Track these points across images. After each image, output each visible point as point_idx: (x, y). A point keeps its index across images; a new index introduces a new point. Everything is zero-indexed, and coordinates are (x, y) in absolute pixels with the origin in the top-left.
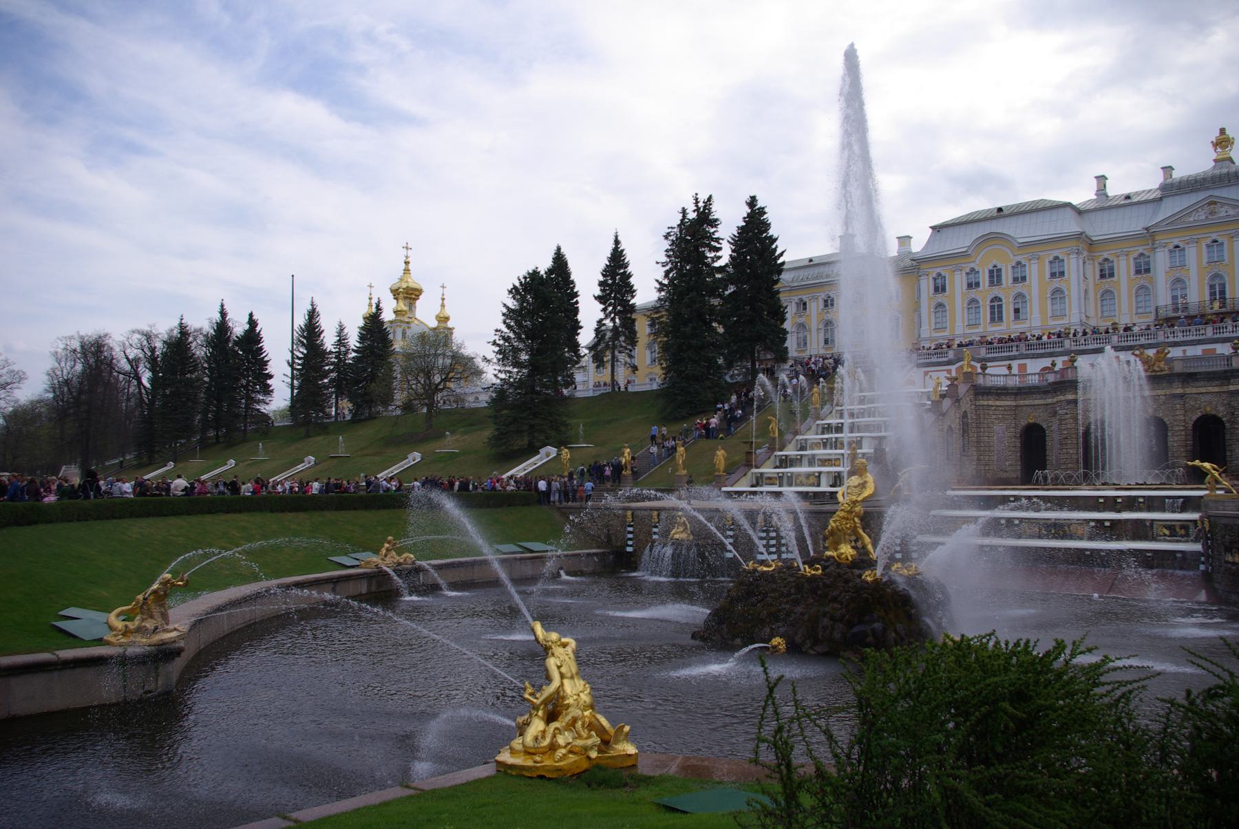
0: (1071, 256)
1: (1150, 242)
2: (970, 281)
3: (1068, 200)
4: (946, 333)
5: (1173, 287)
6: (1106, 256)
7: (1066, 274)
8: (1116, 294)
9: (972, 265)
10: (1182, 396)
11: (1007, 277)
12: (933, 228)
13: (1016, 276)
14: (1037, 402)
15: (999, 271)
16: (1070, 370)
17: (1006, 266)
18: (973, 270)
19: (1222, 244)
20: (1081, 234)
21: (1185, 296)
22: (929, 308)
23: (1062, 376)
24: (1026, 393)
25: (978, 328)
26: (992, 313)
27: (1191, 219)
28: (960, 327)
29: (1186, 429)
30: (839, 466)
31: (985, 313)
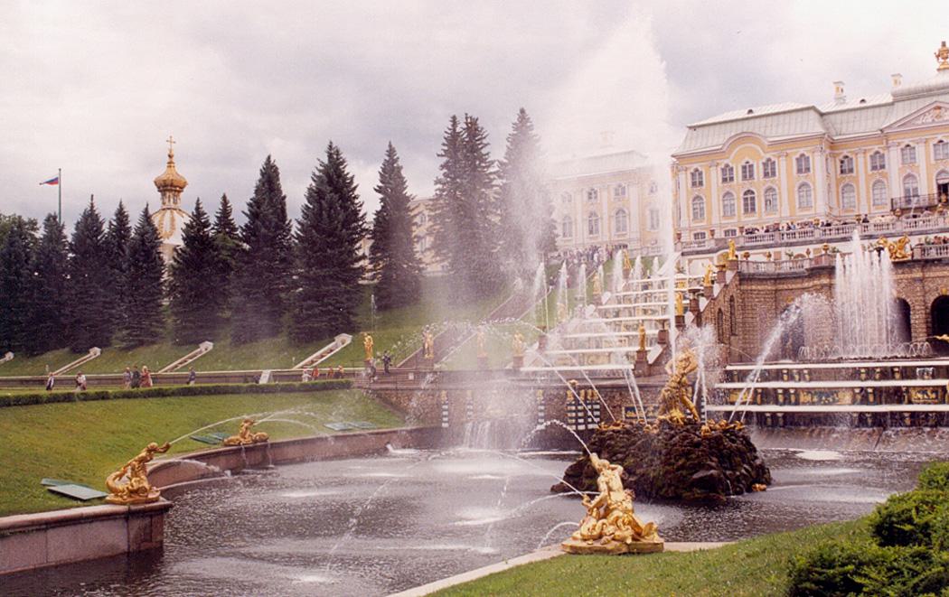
0: (816, 154)
1: (884, 141)
3: (811, 105)
7: (811, 170)
9: (726, 162)
10: (922, 280)
11: (758, 171)
12: (690, 128)
14: (794, 286)
15: (751, 166)
16: (823, 258)
17: (758, 164)
18: (727, 166)
20: (824, 134)
23: (817, 263)
26: (746, 205)
27: (920, 122)
28: (716, 219)
29: (927, 308)
31: (739, 205)
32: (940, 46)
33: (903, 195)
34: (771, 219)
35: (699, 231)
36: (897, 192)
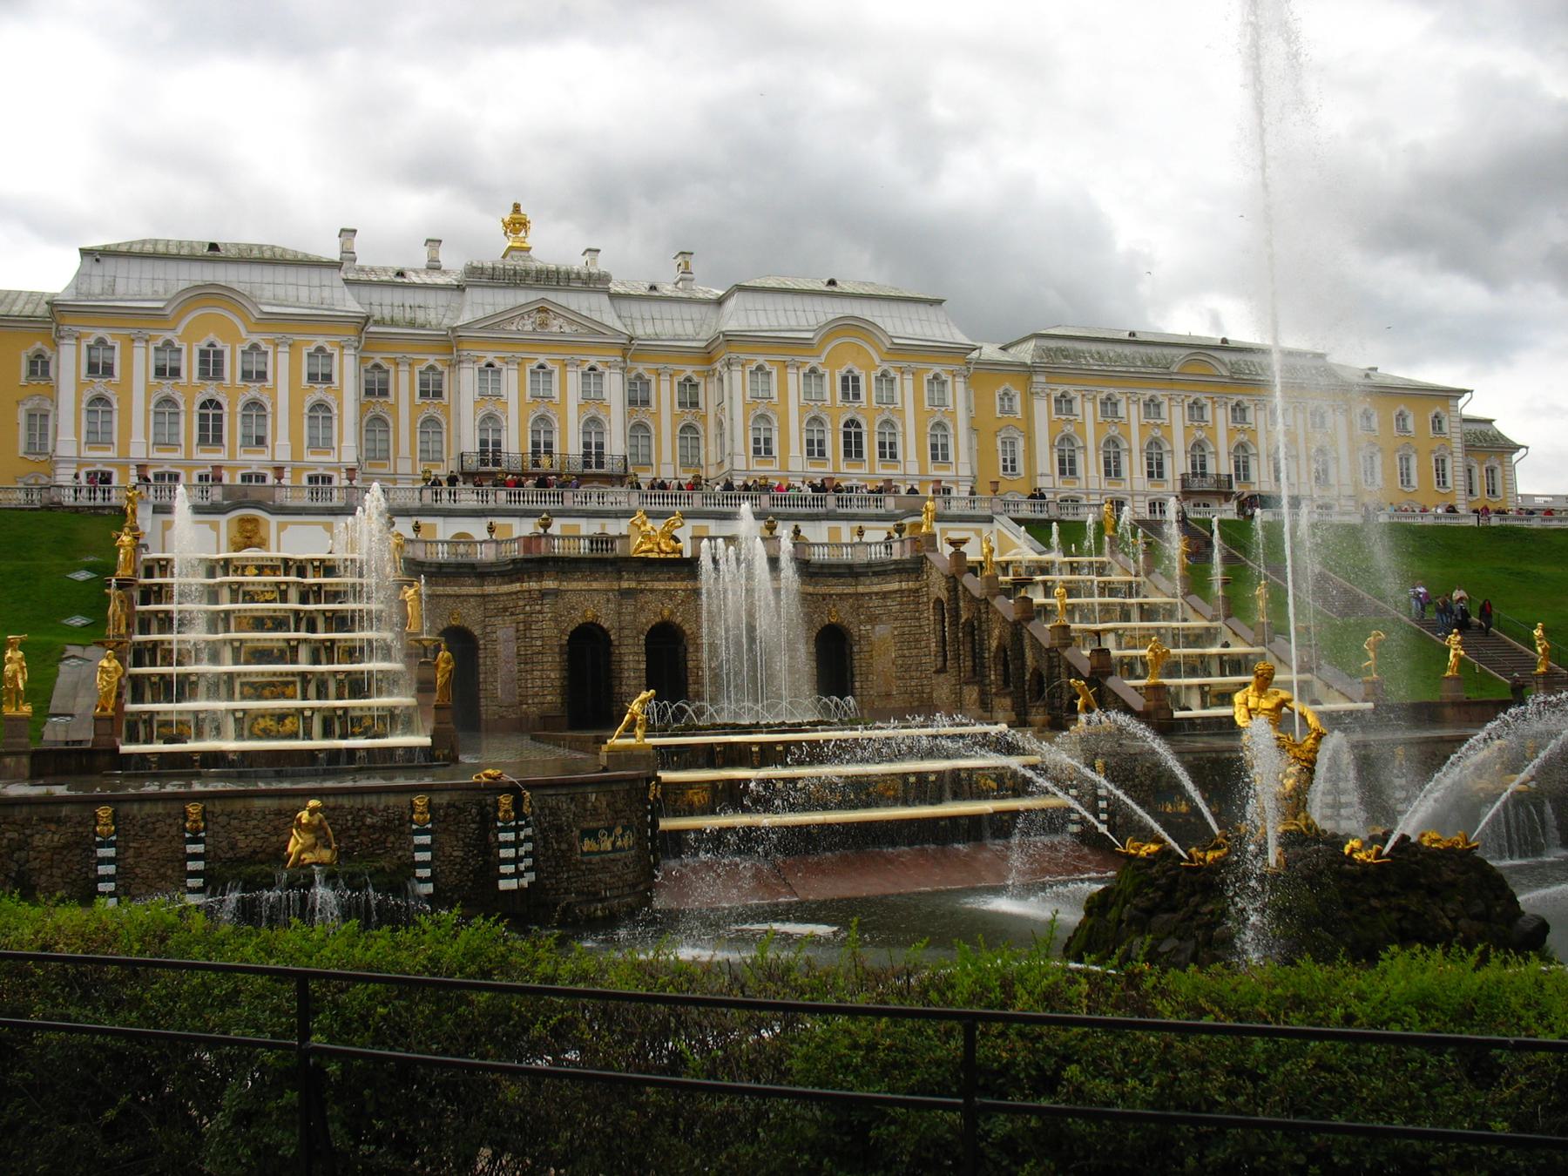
0: (345, 351)
2: (161, 363)
4: (112, 454)
5: (588, 429)
6: (378, 358)
7: (335, 378)
8: (391, 425)
9: (169, 335)
11: (232, 367)
12: (85, 253)
13: (247, 367)
14: (465, 590)
15: (219, 354)
18: (168, 344)
19: (550, 373)
21: (497, 443)
22: (78, 402)
23: (527, 548)
24: (447, 575)
25: (176, 451)
26: (203, 428)
27: (514, 328)
30: (293, 697)
31: (188, 426)
32: (511, 208)
33: (478, 450)
34: (256, 460)
35: (99, 467)
36: (470, 443)
